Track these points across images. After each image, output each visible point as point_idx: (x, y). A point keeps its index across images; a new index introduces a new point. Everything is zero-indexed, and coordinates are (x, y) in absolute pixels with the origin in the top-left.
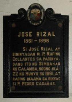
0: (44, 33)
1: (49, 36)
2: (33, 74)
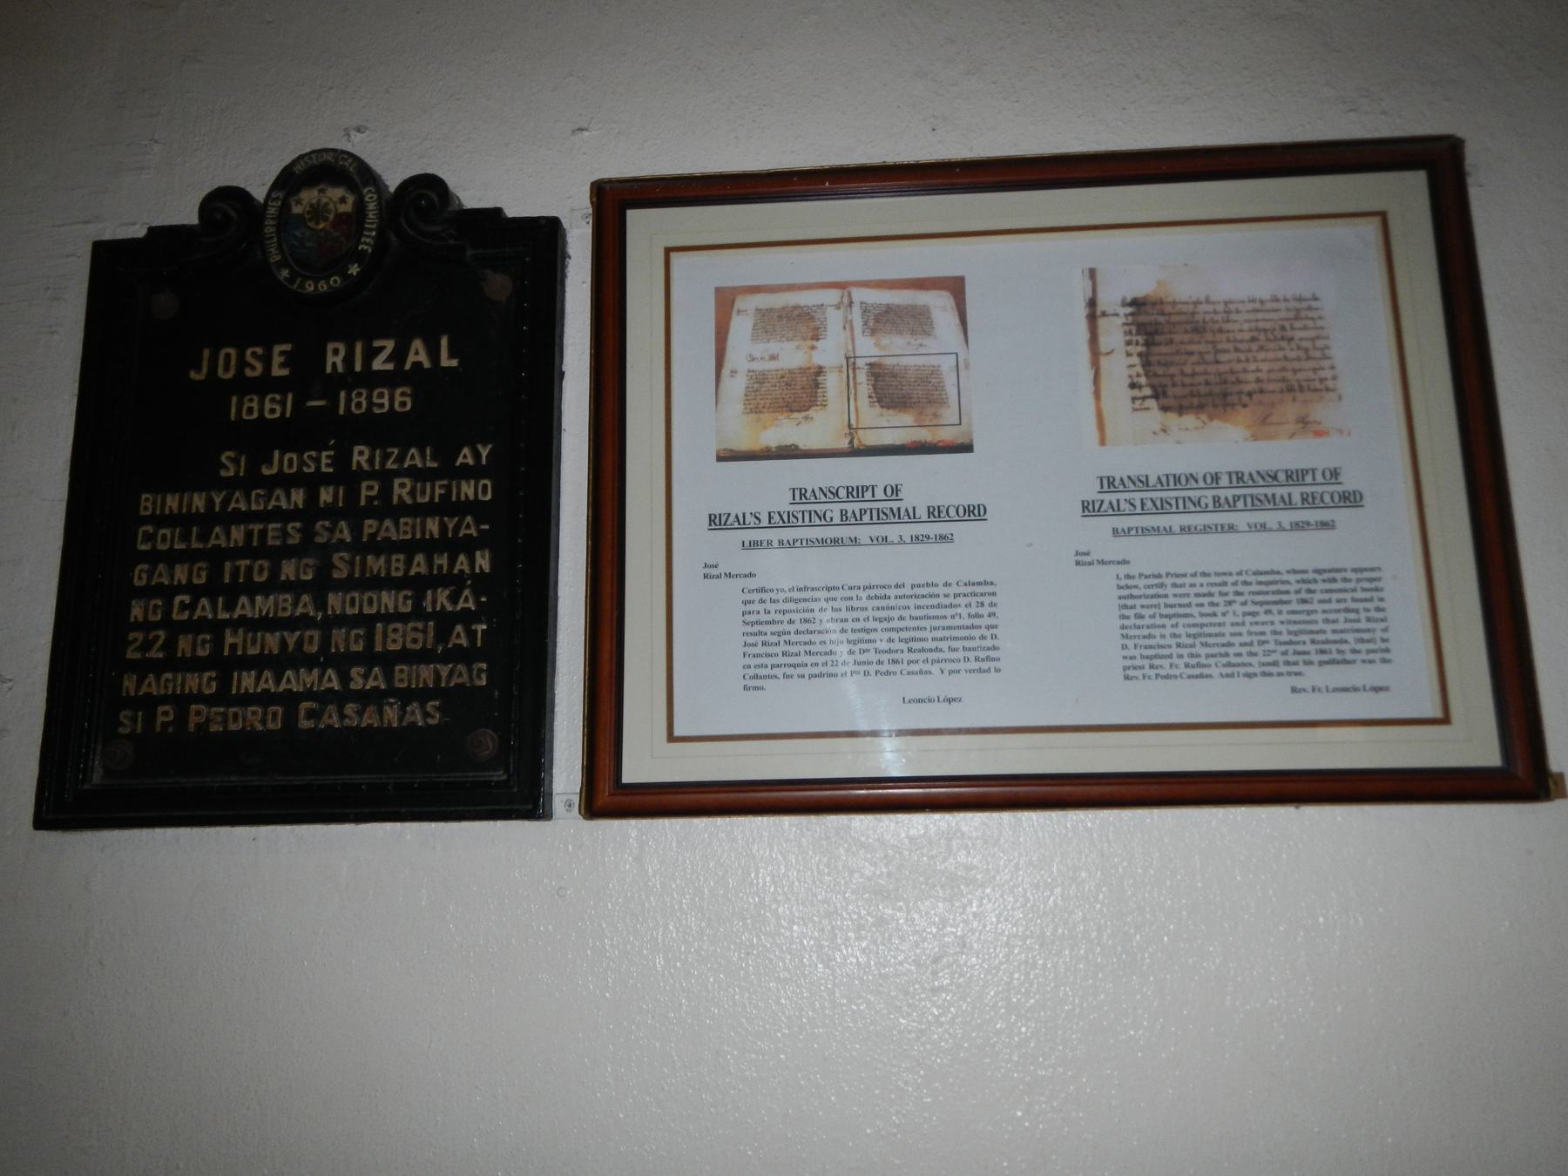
0: (382, 349)
1: (417, 365)
2: (283, 643)
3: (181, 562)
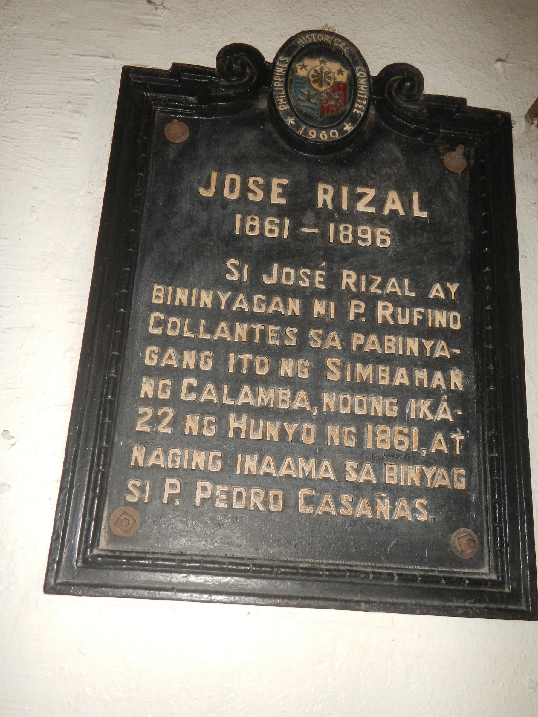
1: (394, 212)
2: (283, 432)
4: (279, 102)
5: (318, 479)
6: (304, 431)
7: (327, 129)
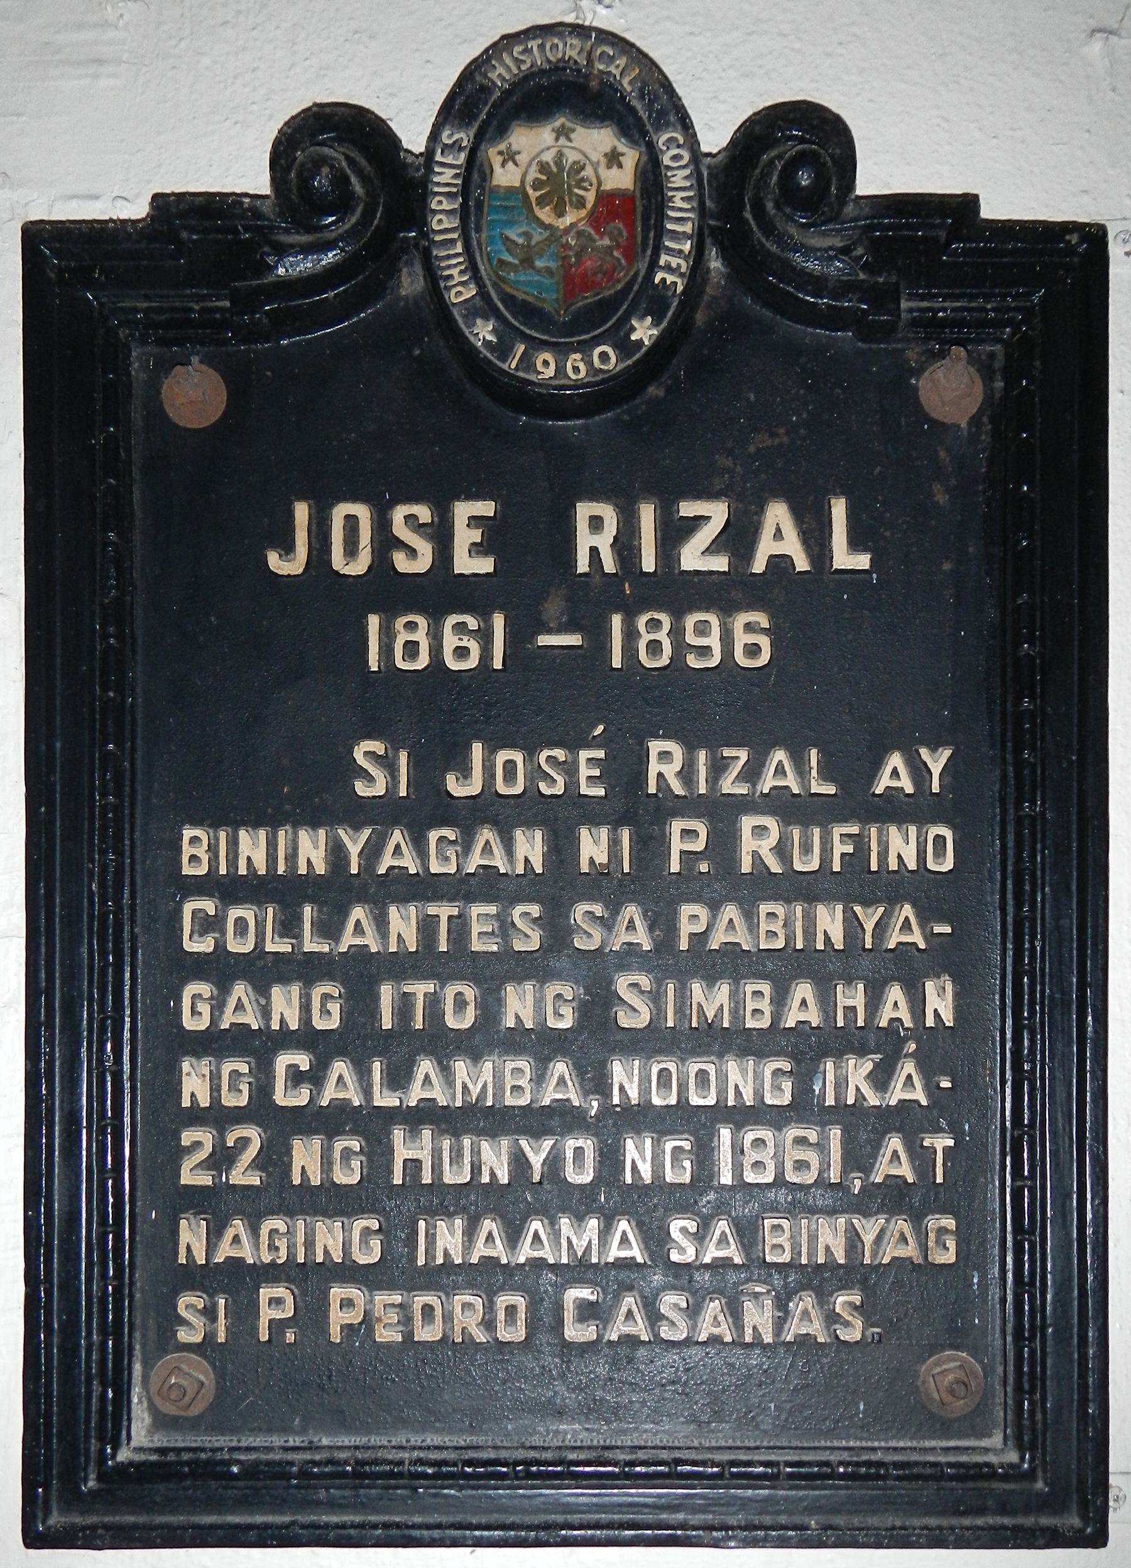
0: (699, 521)
1: (780, 563)
2: (519, 1162)
3: (284, 980)
4: (451, 277)
5: (607, 1264)
6: (569, 1154)
7: (585, 348)
